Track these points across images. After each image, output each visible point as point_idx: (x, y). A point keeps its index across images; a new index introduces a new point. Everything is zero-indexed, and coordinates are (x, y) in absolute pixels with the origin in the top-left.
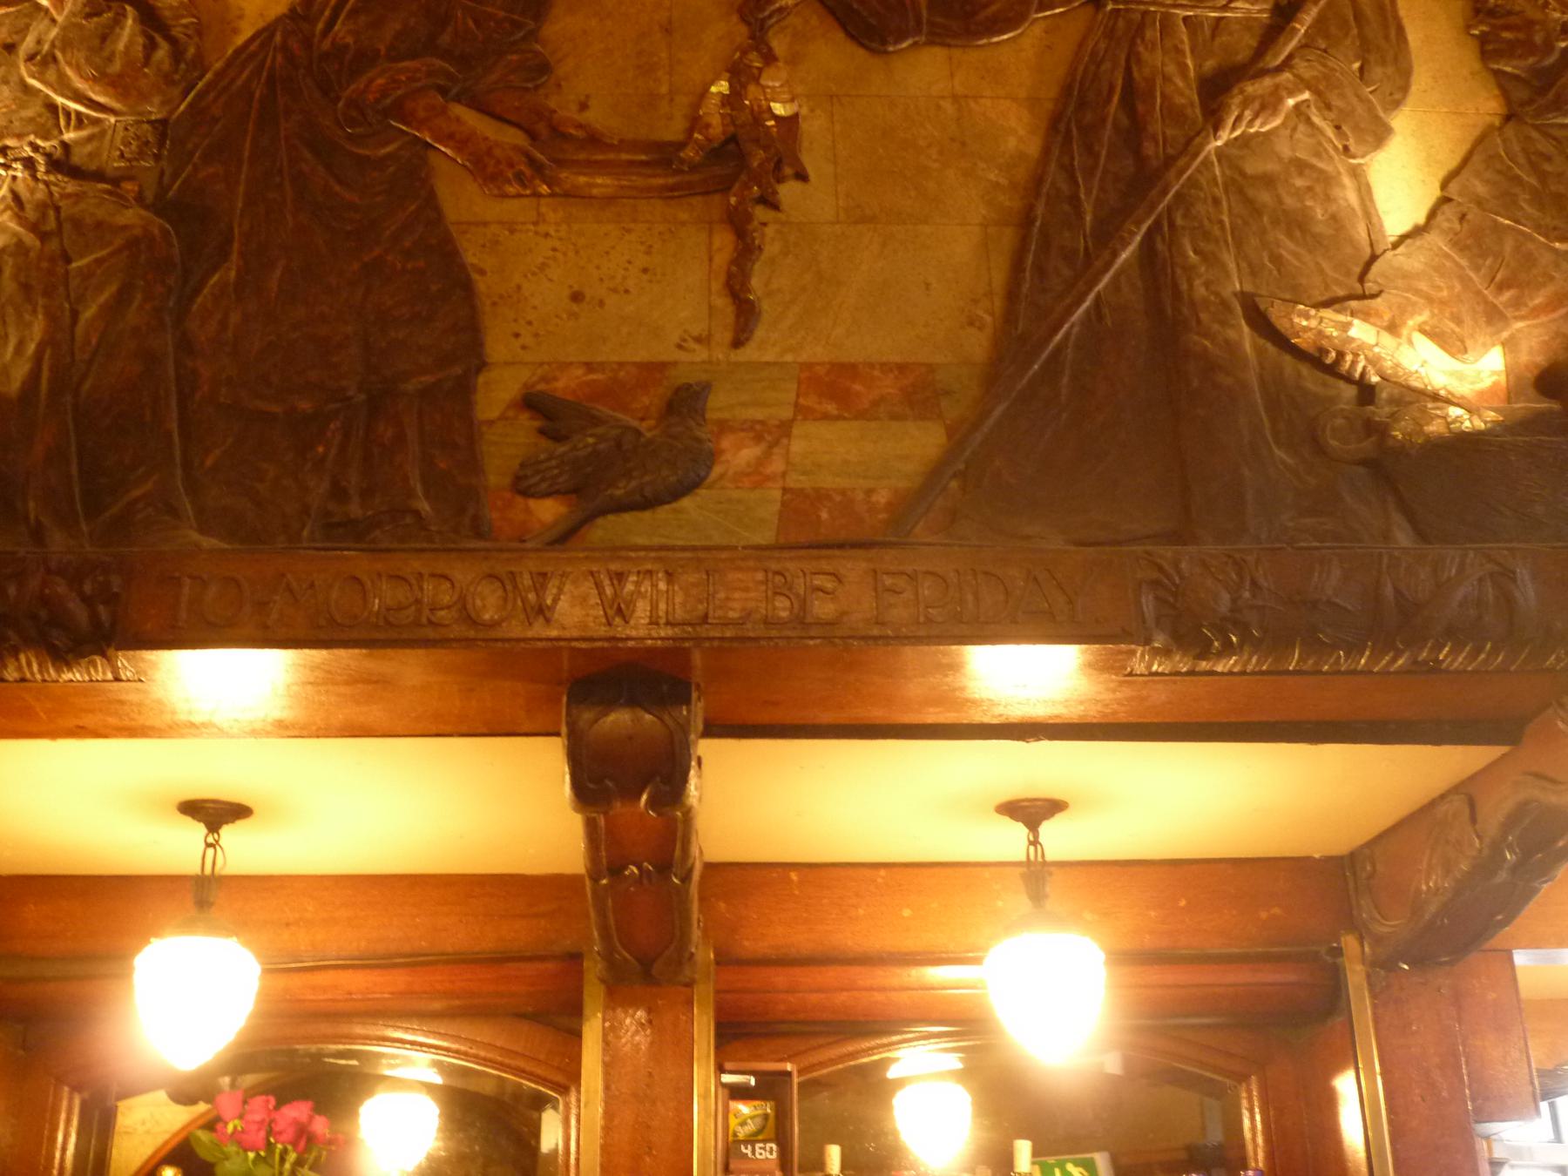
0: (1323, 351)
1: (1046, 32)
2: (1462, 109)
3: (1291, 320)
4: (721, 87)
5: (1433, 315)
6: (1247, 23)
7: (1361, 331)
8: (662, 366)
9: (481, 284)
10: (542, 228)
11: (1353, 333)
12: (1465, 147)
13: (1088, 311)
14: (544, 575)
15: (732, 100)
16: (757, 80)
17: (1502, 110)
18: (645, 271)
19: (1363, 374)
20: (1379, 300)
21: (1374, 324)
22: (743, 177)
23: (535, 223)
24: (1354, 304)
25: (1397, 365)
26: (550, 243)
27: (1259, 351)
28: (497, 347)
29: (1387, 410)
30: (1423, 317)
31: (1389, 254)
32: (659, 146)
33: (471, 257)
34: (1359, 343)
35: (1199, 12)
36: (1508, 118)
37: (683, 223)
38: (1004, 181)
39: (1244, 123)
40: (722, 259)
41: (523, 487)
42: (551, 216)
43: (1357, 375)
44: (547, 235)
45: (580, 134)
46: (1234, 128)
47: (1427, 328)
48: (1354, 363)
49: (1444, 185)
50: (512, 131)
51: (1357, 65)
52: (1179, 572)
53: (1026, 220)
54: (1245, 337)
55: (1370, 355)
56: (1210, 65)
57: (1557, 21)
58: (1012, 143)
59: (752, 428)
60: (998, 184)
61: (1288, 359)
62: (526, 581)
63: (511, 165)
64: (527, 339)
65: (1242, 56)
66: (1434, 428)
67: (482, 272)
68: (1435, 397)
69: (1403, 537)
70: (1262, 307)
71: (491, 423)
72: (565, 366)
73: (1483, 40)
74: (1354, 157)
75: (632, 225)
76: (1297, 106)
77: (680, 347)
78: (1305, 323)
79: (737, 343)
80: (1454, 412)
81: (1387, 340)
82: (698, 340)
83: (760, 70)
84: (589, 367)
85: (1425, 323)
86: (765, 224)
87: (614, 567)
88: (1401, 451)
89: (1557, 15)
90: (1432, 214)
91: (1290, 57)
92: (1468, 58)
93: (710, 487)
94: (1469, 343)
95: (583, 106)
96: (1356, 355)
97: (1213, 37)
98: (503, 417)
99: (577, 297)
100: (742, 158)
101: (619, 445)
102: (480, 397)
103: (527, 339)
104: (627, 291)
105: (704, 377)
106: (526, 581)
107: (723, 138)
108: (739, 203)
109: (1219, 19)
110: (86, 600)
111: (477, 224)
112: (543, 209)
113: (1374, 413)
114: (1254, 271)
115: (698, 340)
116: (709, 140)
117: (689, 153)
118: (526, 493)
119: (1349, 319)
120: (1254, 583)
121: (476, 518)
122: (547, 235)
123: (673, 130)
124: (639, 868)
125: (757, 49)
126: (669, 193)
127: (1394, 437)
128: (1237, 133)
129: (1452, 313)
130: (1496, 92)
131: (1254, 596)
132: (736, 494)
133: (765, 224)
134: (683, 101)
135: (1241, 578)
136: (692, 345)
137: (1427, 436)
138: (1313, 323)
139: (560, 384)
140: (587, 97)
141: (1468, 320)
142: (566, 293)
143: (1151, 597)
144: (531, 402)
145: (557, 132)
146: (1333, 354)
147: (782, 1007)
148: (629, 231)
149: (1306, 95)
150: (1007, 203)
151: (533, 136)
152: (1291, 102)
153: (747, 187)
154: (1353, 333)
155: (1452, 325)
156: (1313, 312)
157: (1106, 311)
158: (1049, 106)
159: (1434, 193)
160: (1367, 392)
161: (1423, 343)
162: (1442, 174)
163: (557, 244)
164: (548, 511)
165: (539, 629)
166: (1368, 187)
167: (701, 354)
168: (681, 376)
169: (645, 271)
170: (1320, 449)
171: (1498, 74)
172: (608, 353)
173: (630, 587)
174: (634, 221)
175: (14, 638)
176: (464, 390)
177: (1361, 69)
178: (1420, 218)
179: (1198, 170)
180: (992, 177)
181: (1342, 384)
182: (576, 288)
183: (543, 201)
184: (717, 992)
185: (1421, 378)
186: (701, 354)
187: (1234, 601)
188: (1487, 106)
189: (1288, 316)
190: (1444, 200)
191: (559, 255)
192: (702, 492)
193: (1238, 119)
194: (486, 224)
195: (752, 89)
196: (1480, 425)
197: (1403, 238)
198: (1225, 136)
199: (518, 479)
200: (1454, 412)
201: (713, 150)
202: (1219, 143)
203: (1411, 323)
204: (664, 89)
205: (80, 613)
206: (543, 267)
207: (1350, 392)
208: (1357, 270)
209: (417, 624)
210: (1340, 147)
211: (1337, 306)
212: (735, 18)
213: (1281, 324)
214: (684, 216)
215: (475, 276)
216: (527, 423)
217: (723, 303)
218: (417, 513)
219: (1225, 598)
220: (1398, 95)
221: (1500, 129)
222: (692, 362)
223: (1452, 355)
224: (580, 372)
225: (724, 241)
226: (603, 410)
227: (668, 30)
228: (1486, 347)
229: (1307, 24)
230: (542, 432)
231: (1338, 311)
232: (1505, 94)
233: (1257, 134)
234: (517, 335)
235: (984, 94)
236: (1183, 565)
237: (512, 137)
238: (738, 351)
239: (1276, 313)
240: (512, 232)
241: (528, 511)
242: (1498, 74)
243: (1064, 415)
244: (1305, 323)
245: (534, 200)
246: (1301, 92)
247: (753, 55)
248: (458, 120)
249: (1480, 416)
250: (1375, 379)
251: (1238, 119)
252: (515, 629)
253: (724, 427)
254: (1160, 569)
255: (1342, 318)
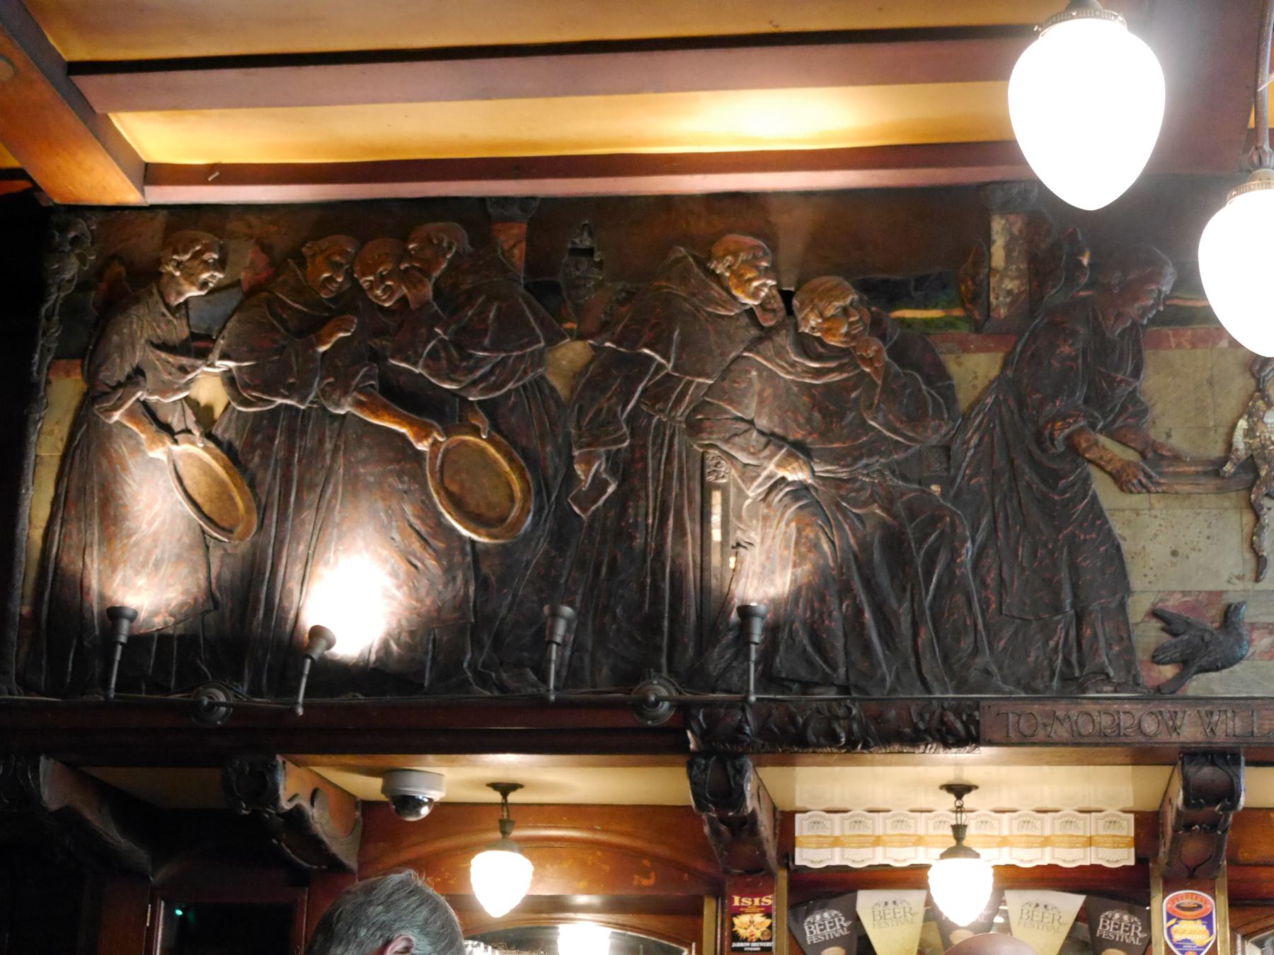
4: (1243, 424)
8: (1220, 593)
9: (1125, 547)
10: (1153, 512)
14: (1176, 712)
15: (1249, 432)
16: (1261, 419)
18: (1208, 538)
22: (1258, 482)
23: (1150, 510)
26: (1158, 522)
28: (1136, 582)
32: (1212, 462)
33: (1117, 531)
37: (1226, 509)
40: (1247, 529)
41: (1156, 659)
42: (1157, 505)
44: (1156, 517)
45: (1168, 454)
50: (1131, 452)
59: (1267, 628)
62: (1167, 716)
63: (1136, 477)
64: (1151, 577)
67: (1125, 539)
71: (1137, 624)
72: (1172, 593)
75: (1199, 511)
77: (1229, 582)
79: (1257, 579)
82: (1238, 578)
83: (1265, 412)
84: (1184, 593)
86: (1269, 509)
87: (1209, 708)
93: (1248, 659)
95: (1169, 435)
98: (1142, 621)
99: (1174, 553)
100: (1256, 470)
101: (1203, 640)
102: (1130, 611)
103: (1151, 577)
104: (1200, 550)
105: (1239, 599)
106: (1167, 716)
107: (1245, 457)
108: (1257, 498)
110: (962, 722)
111: (1119, 510)
112: (1153, 501)
115: (1238, 578)
116: (1239, 459)
117: (1229, 468)
118: (1159, 663)
121: (1134, 677)
122: (1156, 517)
123: (1217, 451)
124: (1200, 826)
125: (1263, 398)
126: (1220, 491)
132: (1261, 663)
133: (1269, 509)
134: (1222, 431)
136: (1235, 580)
139: (1170, 603)
140: (1170, 429)
142: (1168, 551)
144: (1156, 614)
145: (1154, 447)
147: (1265, 890)
148: (1199, 514)
151: (1143, 455)
153: (1259, 488)
163: (1162, 522)
164: (1168, 671)
165: (1174, 738)
167: (1240, 586)
168: (1233, 598)
169: (1208, 538)
172: (1192, 586)
173: (1216, 718)
174: (1201, 507)
175: (930, 739)
176: (1122, 606)
182: (1174, 548)
183: (1153, 495)
184: (1229, 881)
186: (1240, 586)
191: (1163, 529)
192: (1244, 662)
194: (1123, 510)
195: (1260, 424)
199: (1154, 657)
201: (1241, 464)
204: (1211, 424)
205: (959, 726)
206: (1156, 535)
209: (1119, 735)
212: (1248, 375)
214: (1227, 504)
215: (1122, 542)
216: (1156, 624)
217: (1249, 556)
218: (1107, 675)
222: (1235, 591)
224: (1179, 596)
225: (1248, 518)
226: (1192, 618)
227: (1211, 383)
230: (1163, 629)
234: (1146, 576)
237: (1132, 456)
238: (1261, 583)
240: (1138, 515)
241: (1160, 672)
245: (1147, 496)
247: (1260, 403)
248: (1104, 448)
252: (1163, 737)
253: (1253, 626)
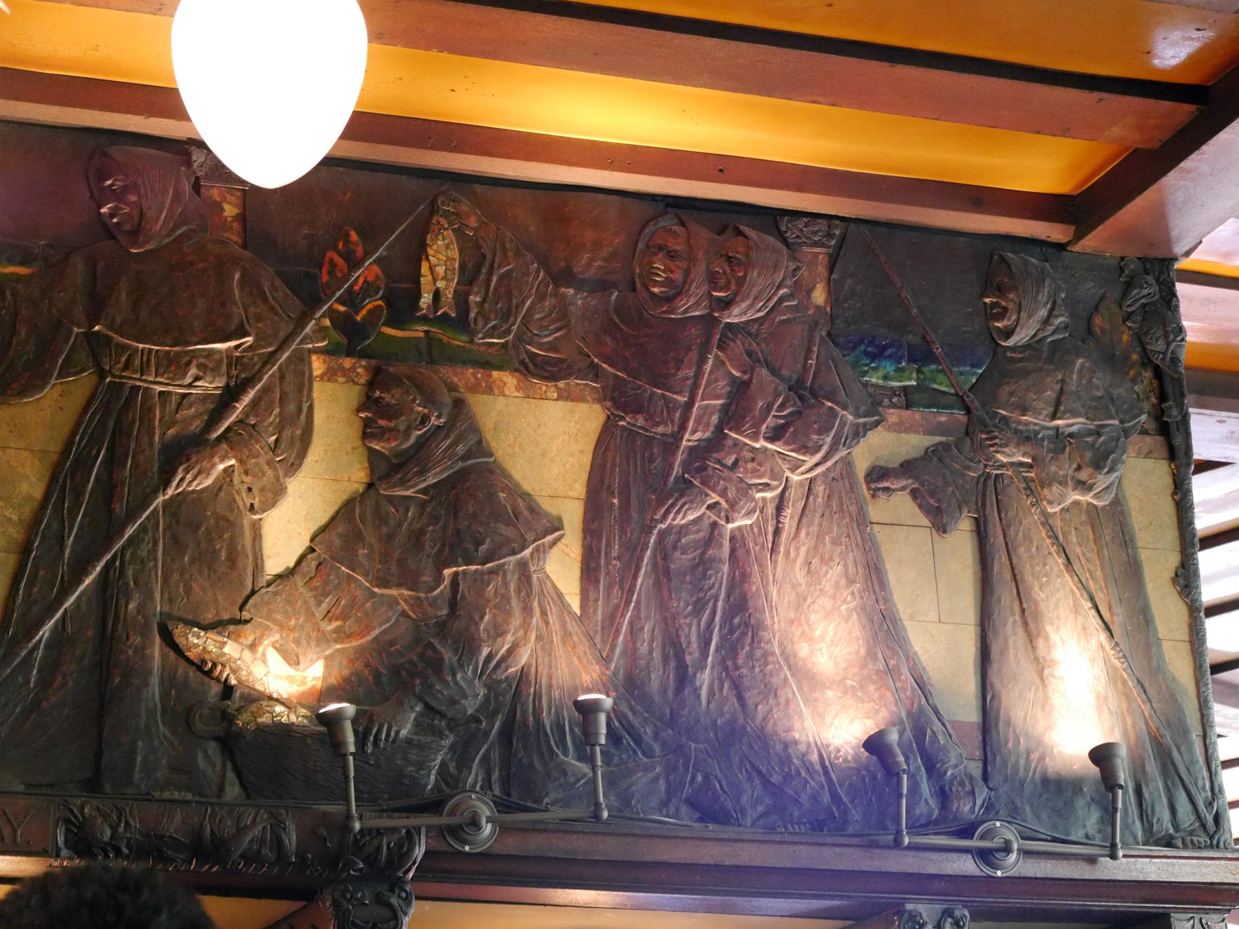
0: (204, 662)
1: (61, 396)
2: (339, 478)
3: (187, 639)
5: (282, 637)
6: (205, 398)
7: (231, 649)
11: (226, 650)
12: (335, 508)
13: (57, 621)
17: (366, 480)
19: (226, 680)
20: (249, 625)
21: (241, 644)
24: (232, 628)
25: (250, 673)
27: (164, 657)
29: (237, 705)
30: (277, 636)
31: (264, 590)
34: (228, 656)
35: (170, 389)
36: (370, 486)
38: (15, 517)
39: (185, 484)
43: (223, 680)
46: (178, 486)
47: (277, 646)
48: (221, 672)
49: (312, 540)
51: (274, 438)
52: (83, 814)
53: (25, 550)
54: (157, 648)
55: (234, 666)
56: (171, 432)
57: (418, 413)
58: (24, 488)
60: (10, 519)
61: (182, 663)
65: (196, 426)
66: (265, 719)
68: (270, 698)
69: (233, 790)
70: (170, 628)
73: (367, 423)
74: (255, 513)
76: (225, 470)
78: (196, 641)
80: (279, 709)
81: (247, 655)
85: (277, 642)
88: (240, 735)
89: (420, 409)
90: (299, 562)
91: (228, 429)
92: (354, 431)
94: (301, 658)
96: (224, 666)
97: (177, 412)
109: (184, 396)
113: (228, 706)
114: (171, 601)
119: (225, 639)
120: (127, 823)
127: (237, 725)
128: (180, 490)
129: (294, 638)
130: (366, 465)
131: (126, 830)
135: (120, 821)
137: (257, 724)
138: (200, 642)
141: (304, 642)
143: (63, 829)
146: (210, 665)
149: (233, 462)
150: (15, 535)
152: (221, 467)
154: (226, 650)
155: (293, 645)
156: (202, 634)
157: (68, 621)
158: (54, 458)
159: (306, 543)
160: (228, 690)
161: (273, 656)
162: (313, 528)
166: (260, 535)
170: (189, 725)
171: (371, 451)
177: (277, 441)
178: (292, 565)
179: (148, 518)
180: (7, 513)
181: (213, 683)
185: (263, 684)
187: (113, 834)
188: (356, 476)
189: (186, 635)
190: (311, 550)
193: (182, 480)
196: (293, 718)
197: (279, 577)
198: (170, 492)
200: (279, 709)
202: (167, 497)
203: (266, 643)
207: (215, 689)
208: (240, 601)
210: (248, 505)
211: (220, 629)
213: (181, 641)
219: (108, 832)
220: (294, 467)
221: (363, 494)
223: (289, 664)
228: (313, 662)
229: (245, 404)
231: (219, 633)
232: (372, 468)
233: (194, 491)
235: (11, 445)
236: (86, 811)
239: (178, 631)
242: (371, 451)
243: (31, 696)
244: (196, 641)
246: (229, 459)
249: (295, 712)
250: (233, 682)
251: (182, 480)
254: (72, 811)
255: (220, 639)
